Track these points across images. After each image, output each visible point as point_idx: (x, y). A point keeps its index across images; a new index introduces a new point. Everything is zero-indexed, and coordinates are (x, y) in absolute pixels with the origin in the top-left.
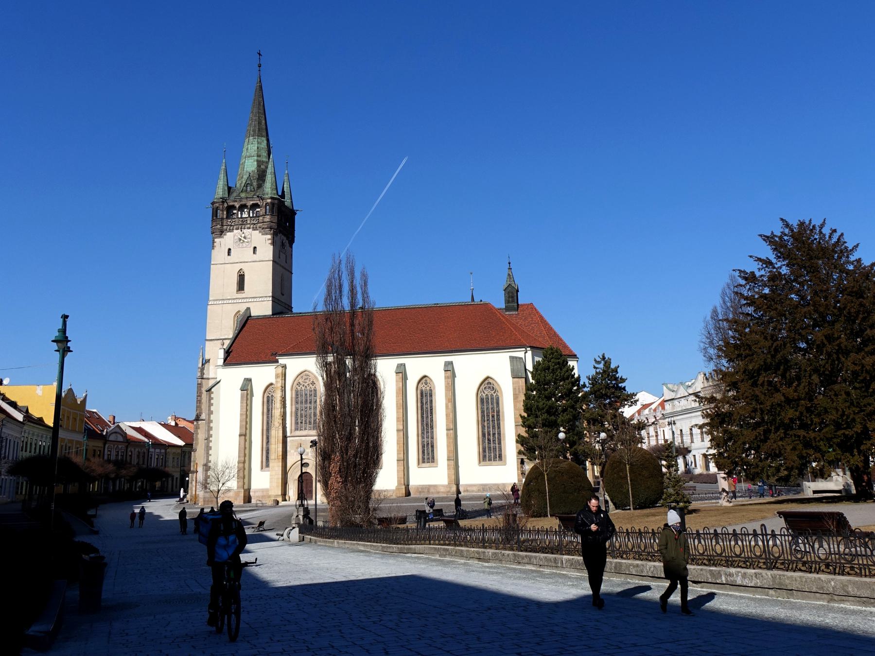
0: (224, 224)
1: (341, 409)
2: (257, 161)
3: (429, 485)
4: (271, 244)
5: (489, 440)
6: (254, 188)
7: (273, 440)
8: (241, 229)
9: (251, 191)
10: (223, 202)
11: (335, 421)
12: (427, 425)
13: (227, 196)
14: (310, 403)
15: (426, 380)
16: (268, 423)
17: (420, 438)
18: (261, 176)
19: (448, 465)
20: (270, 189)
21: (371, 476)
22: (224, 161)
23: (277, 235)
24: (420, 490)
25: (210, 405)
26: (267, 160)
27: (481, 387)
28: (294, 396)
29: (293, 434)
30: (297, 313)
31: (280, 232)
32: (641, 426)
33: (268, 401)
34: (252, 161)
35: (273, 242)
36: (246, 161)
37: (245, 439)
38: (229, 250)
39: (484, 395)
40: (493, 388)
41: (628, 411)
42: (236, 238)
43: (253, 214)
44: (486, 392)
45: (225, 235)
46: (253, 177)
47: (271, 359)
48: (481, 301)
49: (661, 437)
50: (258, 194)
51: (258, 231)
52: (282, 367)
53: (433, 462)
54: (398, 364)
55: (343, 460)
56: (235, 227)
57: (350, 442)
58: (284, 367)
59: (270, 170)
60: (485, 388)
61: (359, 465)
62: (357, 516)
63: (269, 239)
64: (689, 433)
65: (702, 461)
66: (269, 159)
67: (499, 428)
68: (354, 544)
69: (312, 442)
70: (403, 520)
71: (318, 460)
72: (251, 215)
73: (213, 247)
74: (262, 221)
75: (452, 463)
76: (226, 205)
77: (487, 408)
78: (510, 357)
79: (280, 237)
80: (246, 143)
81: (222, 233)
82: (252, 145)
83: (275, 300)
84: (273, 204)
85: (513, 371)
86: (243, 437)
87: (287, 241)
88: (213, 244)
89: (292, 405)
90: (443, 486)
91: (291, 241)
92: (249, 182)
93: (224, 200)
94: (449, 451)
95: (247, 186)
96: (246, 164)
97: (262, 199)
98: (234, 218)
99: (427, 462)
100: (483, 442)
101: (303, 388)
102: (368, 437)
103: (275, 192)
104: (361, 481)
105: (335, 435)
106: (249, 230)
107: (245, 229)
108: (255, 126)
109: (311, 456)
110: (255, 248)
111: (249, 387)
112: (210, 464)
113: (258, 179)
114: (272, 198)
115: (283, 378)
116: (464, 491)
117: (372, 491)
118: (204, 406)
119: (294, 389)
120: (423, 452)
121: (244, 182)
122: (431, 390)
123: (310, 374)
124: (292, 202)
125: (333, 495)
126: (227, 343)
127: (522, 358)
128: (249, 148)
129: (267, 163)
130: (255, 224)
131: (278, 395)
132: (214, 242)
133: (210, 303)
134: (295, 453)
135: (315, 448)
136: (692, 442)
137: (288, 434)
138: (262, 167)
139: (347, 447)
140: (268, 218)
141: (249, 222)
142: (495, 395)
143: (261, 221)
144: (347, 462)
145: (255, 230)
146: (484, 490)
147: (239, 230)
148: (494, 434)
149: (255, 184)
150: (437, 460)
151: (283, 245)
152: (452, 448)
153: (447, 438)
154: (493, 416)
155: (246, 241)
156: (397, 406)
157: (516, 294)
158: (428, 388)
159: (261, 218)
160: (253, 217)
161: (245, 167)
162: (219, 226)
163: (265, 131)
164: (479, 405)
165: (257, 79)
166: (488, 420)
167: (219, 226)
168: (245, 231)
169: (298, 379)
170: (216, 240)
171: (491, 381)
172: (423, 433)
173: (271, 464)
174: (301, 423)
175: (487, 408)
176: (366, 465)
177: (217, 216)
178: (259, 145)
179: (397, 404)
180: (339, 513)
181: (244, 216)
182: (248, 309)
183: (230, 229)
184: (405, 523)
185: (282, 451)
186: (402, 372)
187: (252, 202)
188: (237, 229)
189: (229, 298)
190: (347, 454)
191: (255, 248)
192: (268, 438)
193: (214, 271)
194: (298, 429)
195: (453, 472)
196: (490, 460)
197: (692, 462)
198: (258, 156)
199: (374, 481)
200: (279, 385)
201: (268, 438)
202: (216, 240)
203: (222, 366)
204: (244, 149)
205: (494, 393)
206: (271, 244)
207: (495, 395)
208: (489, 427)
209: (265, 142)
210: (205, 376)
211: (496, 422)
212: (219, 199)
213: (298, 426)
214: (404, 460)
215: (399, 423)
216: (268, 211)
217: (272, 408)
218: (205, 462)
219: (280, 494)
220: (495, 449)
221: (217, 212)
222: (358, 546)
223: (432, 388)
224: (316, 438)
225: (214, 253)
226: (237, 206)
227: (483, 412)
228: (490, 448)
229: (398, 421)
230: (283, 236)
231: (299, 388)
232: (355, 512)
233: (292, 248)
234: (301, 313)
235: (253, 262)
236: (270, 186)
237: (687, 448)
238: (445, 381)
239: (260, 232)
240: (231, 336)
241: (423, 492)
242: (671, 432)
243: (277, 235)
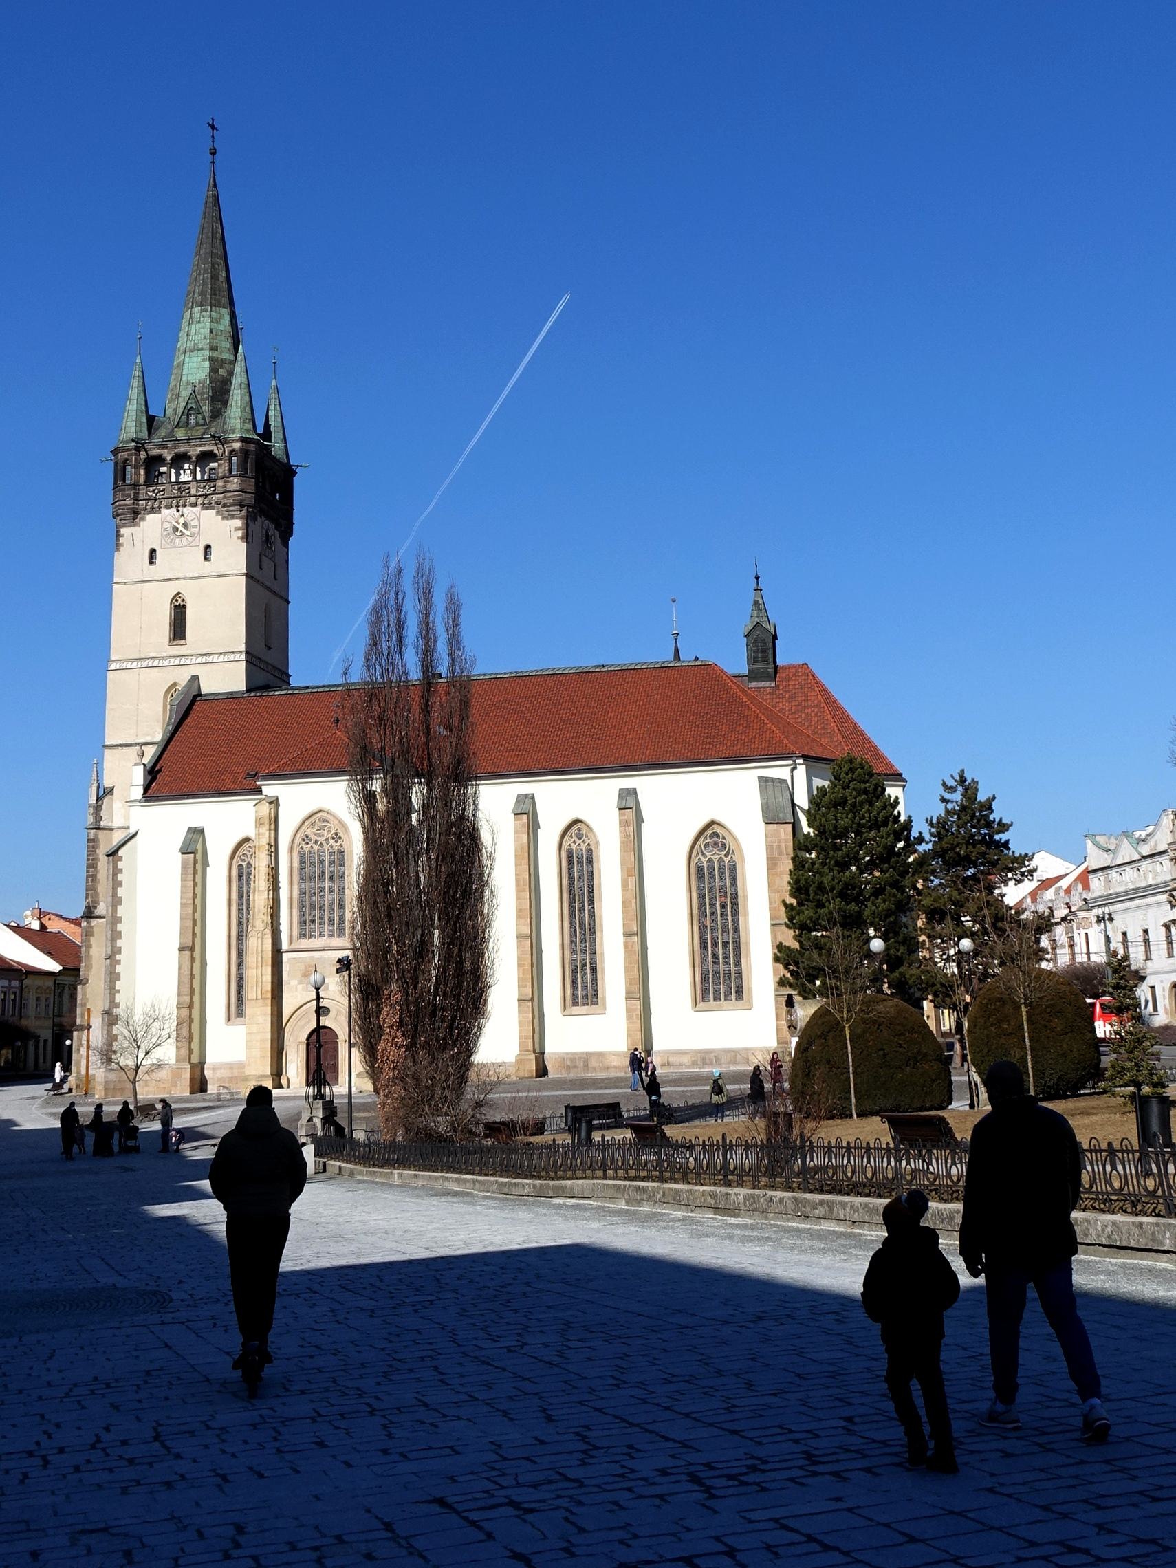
0: (141, 497)
1: (401, 889)
2: (211, 359)
3: (587, 1053)
4: (242, 538)
5: (715, 956)
6: (204, 419)
7: (251, 959)
8: (178, 506)
9: (197, 424)
10: (137, 449)
11: (389, 916)
12: (582, 924)
13: (146, 437)
14: (331, 879)
15: (579, 830)
16: (240, 923)
17: (567, 952)
18: (219, 392)
19: (628, 1010)
20: (238, 421)
21: (467, 1033)
22: (138, 360)
23: (255, 520)
25: (116, 884)
26: (232, 358)
27: (698, 844)
28: (296, 864)
30: (300, 688)
31: (262, 513)
32: (1044, 924)
33: (240, 876)
34: (200, 359)
35: (247, 535)
36: (187, 360)
37: (192, 955)
38: (153, 551)
39: (704, 860)
40: (724, 845)
41: (1013, 893)
42: (167, 525)
43: (203, 475)
44: (709, 855)
45: (143, 519)
46: (202, 394)
47: (246, 786)
48: (696, 659)
49: (1080, 948)
50: (212, 430)
51: (214, 511)
52: (270, 803)
53: (595, 1003)
54: (519, 796)
55: (407, 1000)
56: (164, 503)
57: (423, 961)
58: (275, 802)
59: (238, 379)
60: (707, 845)
61: (443, 1009)
62: (439, 1119)
63: (237, 529)
64: (1141, 939)
65: (1170, 998)
66: (236, 356)
67: (736, 930)
68: (437, 1179)
69: (339, 961)
70: (539, 1128)
71: (353, 1000)
72: (199, 477)
74: (222, 490)
75: (637, 1005)
76: (143, 455)
77: (711, 889)
78: (761, 779)
79: (262, 523)
80: (185, 321)
81: (135, 515)
82: (197, 325)
83: (253, 659)
84: (245, 453)
85: (766, 809)
86: (188, 953)
87: (277, 533)
88: (118, 540)
89: (291, 883)
90: (617, 1054)
91: (286, 531)
92: (193, 406)
93: (139, 445)
94: (629, 982)
95: (188, 415)
96: (186, 366)
97: (223, 442)
98: (163, 484)
99: (583, 1005)
100: (703, 959)
101: (316, 848)
102: (460, 950)
103: (250, 426)
104: (447, 1043)
105: (390, 947)
106: (194, 509)
107: (185, 506)
108: (204, 284)
109: (338, 995)
110: (208, 547)
111: (199, 847)
112: (117, 1011)
113: (213, 399)
116: (663, 1065)
117: (471, 1065)
118: (103, 888)
120: (574, 982)
121: (183, 405)
122: (590, 851)
124: (286, 447)
125: (388, 1073)
126: (150, 753)
127: (785, 781)
128: (193, 332)
129: (233, 363)
130: (206, 496)
131: (261, 863)
133: (112, 667)
134: (300, 987)
135: (346, 974)
136: (1148, 958)
137: (285, 946)
138: (222, 372)
139: (415, 971)
140: (234, 483)
141: (193, 491)
142: (727, 860)
143: (219, 489)
144: (416, 1003)
145: (206, 509)
146: (704, 1063)
147: (174, 510)
148: (726, 944)
149: (206, 409)
150: (604, 998)
151: (268, 540)
152: (636, 973)
153: (626, 952)
154: (723, 906)
155: (187, 533)
156: (517, 885)
157: (771, 645)
158: (584, 847)
159: (220, 483)
160: (202, 481)
161: (185, 372)
162: (129, 502)
163: (226, 294)
164: (694, 882)
165: (206, 182)
166: (712, 914)
167: (129, 502)
168: (186, 511)
170: (123, 531)
171: (718, 830)
172: (573, 942)
173: (248, 1010)
174: (313, 921)
175: (711, 889)
176: (457, 1011)
177: (124, 480)
178: (214, 326)
179: (517, 881)
180: (401, 1113)
181: (183, 478)
183: (153, 508)
184: (542, 1134)
185: (272, 983)
186: (527, 811)
187: (199, 449)
188: (169, 507)
190: (415, 987)
191: (208, 547)
192: (240, 954)
194: (305, 936)
195: (638, 1024)
196: (717, 998)
197: (1147, 1002)
198: (211, 349)
199: (475, 1045)
200: (264, 841)
201: (240, 954)
202: (123, 531)
203: (140, 801)
204: (183, 334)
205: (726, 855)
206: (242, 538)
207: (727, 860)
208: (714, 930)
209: (227, 318)
210: (103, 824)
211: (730, 918)
212: (127, 442)
213: (305, 928)
214: (532, 1000)
215: (522, 921)
216: (234, 467)
217: (248, 892)
218: (107, 1007)
219: (269, 1073)
220: (728, 974)
221: (125, 469)
222: (446, 1183)
223: (592, 847)
224: (349, 953)
225: (121, 559)
226: (169, 458)
227: (701, 896)
228: (716, 973)
229: (519, 917)
230: (267, 522)
231: (307, 848)
232: (437, 1112)
233: (287, 547)
234: (308, 688)
235: (204, 577)
236: (238, 414)
237: (1137, 972)
238: (620, 832)
239: (218, 513)
240: (158, 737)
241: (575, 1067)
242: (1102, 937)
243: (255, 520)
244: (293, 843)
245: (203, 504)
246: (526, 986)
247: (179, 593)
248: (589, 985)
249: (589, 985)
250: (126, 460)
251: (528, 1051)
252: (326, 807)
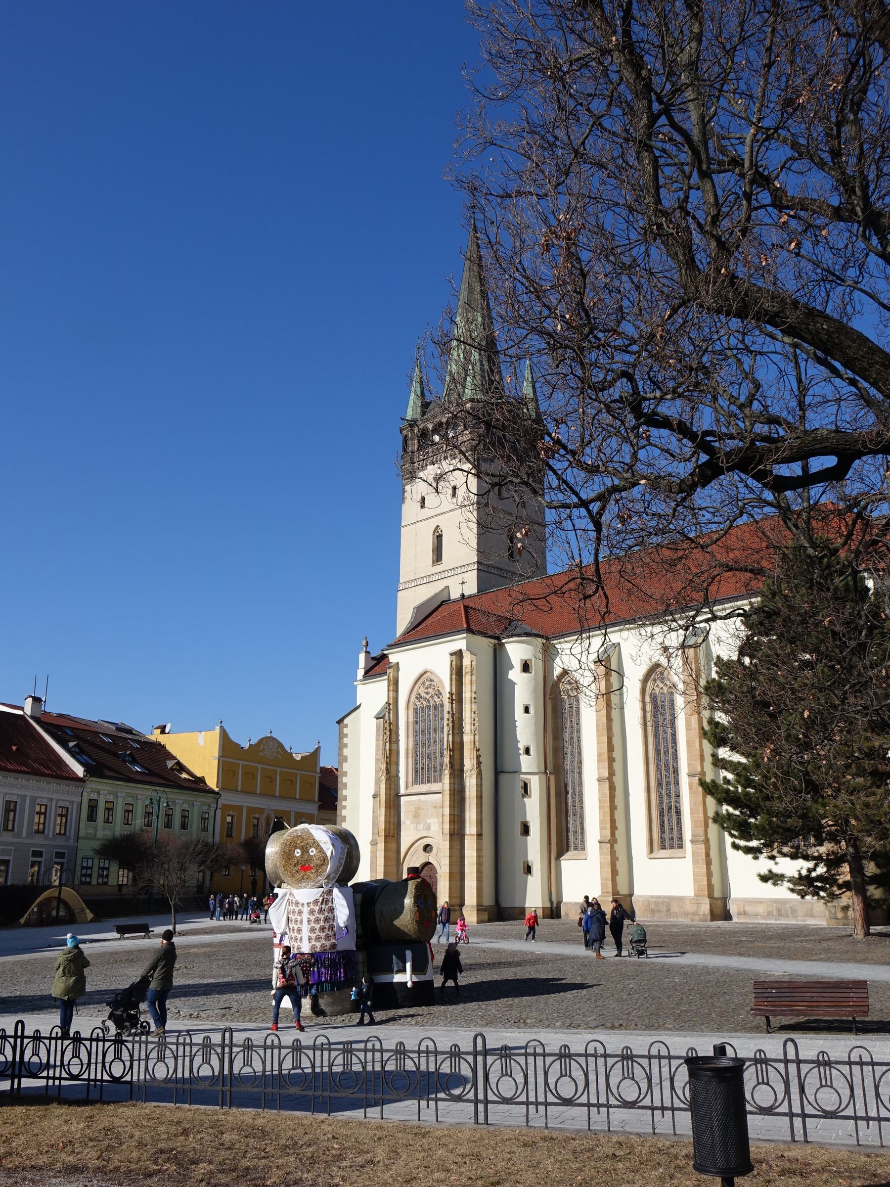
0: (415, 460)
10: (411, 426)
12: (667, 766)
24: (653, 906)
28: (411, 720)
29: (410, 791)
73: (403, 500)
81: (412, 476)
93: (412, 424)
114: (472, 400)
115: (391, 688)
116: (739, 914)
119: (412, 706)
123: (433, 677)
132: (404, 491)
137: (402, 791)
146: (780, 914)
156: (598, 731)
169: (417, 686)
174: (423, 769)
179: (598, 726)
182: (447, 587)
189: (423, 575)
193: (406, 534)
213: (420, 775)
229: (599, 761)
244: (409, 701)
245: (451, 456)
246: (605, 828)
247: (438, 526)
248: (675, 828)
249: (675, 828)
250: (406, 436)
251: (608, 892)
252: (429, 668)
